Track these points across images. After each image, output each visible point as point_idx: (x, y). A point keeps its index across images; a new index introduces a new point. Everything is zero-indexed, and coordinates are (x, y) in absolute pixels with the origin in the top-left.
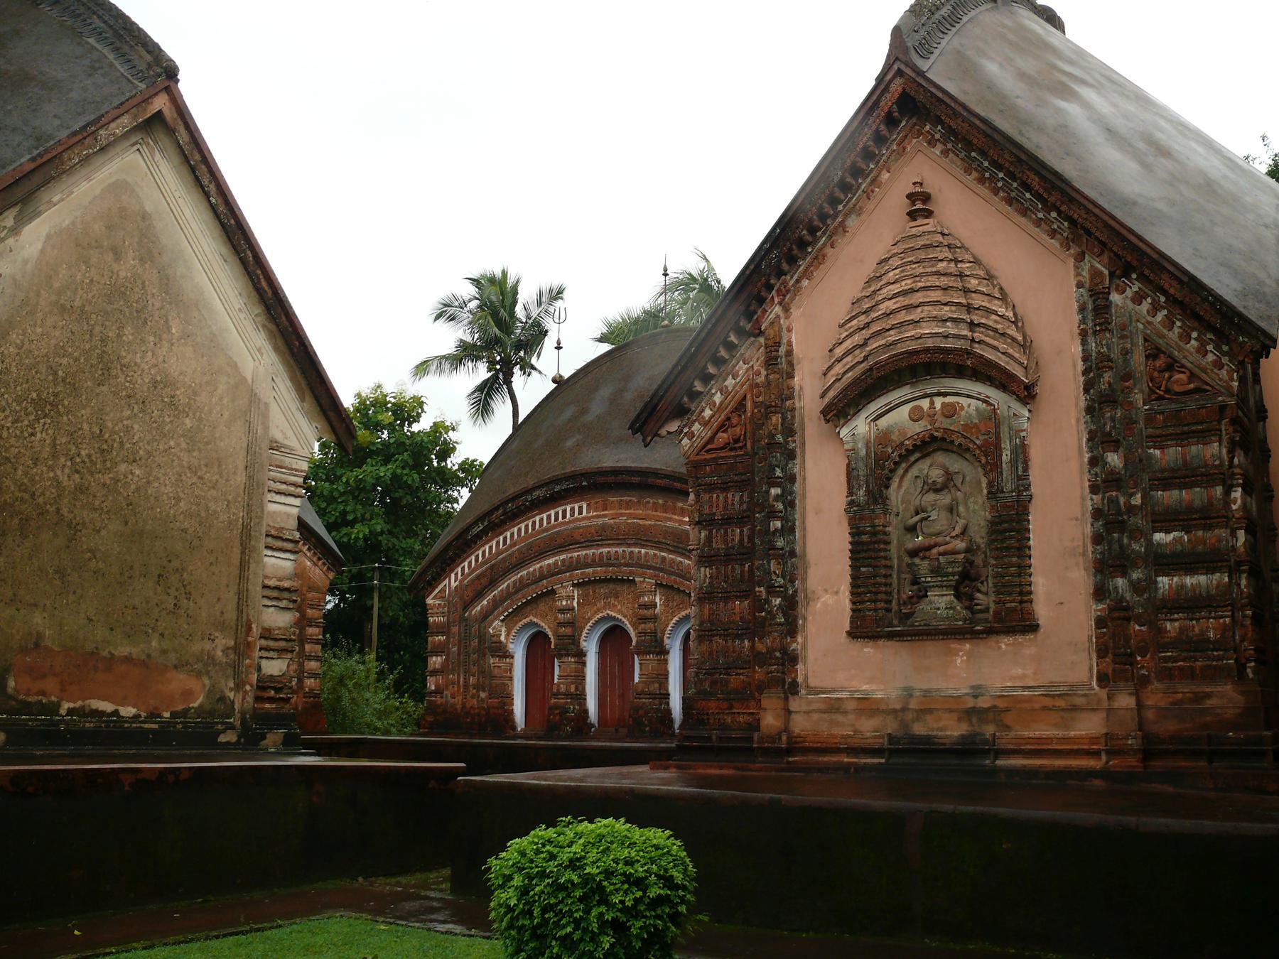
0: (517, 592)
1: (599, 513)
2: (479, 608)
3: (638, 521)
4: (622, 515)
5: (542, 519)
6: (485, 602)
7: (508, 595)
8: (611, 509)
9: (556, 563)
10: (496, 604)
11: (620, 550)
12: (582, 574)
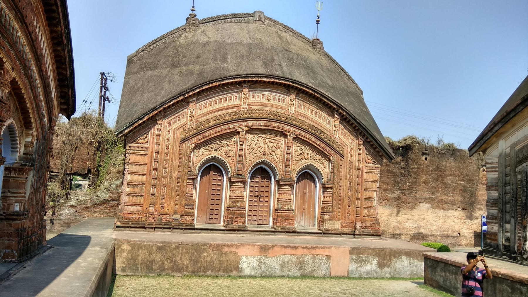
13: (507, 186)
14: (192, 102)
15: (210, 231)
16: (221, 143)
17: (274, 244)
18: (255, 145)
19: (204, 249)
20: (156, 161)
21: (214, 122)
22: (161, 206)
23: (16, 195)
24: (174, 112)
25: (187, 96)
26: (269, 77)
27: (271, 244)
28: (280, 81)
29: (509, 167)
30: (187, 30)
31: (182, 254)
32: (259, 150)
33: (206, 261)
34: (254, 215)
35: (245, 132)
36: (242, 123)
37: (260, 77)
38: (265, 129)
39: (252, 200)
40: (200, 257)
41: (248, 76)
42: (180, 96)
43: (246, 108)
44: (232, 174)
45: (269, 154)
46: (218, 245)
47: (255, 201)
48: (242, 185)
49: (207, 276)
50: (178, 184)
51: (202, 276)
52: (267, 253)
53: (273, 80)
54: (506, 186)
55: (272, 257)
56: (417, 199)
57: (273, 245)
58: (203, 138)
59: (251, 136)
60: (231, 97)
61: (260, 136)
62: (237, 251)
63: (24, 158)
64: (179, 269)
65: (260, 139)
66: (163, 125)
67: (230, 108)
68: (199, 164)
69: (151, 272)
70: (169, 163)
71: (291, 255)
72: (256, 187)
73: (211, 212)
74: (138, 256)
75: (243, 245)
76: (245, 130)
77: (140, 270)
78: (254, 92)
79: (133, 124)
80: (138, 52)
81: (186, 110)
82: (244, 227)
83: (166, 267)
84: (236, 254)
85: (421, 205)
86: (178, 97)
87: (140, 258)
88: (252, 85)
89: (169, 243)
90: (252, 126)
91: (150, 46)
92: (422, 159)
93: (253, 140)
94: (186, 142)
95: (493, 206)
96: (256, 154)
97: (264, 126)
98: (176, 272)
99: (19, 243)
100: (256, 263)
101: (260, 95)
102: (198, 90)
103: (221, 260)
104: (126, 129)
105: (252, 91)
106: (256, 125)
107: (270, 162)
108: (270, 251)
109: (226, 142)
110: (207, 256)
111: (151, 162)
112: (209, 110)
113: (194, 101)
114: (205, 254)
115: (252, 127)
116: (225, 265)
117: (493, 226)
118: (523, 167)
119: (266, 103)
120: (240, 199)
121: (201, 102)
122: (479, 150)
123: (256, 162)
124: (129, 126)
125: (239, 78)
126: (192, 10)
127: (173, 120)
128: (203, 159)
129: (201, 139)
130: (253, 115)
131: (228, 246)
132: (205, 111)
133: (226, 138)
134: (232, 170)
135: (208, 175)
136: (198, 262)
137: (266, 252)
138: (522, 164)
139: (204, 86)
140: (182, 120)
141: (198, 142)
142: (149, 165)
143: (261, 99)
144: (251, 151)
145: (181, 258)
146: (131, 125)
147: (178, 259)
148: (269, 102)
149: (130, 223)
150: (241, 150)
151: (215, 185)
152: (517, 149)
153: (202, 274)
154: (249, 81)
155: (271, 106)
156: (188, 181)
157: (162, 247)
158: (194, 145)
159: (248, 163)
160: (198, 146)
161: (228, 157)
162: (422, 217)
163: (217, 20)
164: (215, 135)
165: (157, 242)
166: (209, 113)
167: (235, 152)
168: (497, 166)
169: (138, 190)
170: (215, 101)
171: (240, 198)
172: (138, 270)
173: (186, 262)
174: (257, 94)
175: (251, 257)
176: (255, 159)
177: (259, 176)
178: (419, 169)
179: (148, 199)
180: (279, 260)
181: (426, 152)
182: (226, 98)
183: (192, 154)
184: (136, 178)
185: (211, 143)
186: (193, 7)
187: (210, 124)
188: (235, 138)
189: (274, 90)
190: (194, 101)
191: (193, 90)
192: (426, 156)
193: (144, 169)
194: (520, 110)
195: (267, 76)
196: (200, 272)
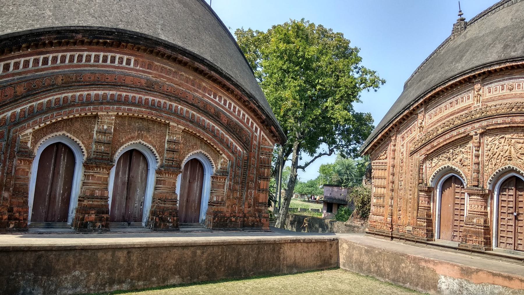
0: (61, 108)
1: (144, 69)
2: (9, 114)
3: (174, 85)
4: (163, 77)
5: (90, 56)
6: (18, 110)
7: (49, 109)
8: (155, 70)
9: (105, 96)
10: (32, 114)
11: (163, 101)
12: (128, 110)
14: (420, 113)
15: (441, 248)
16: (455, 151)
17: (479, 268)
18: (497, 149)
19: (402, 259)
20: (393, 175)
21: (443, 129)
22: (398, 217)
23: (216, 192)
24: (407, 126)
25: (412, 108)
26: (502, 63)
27: (473, 267)
28: (519, 63)
30: (452, 38)
31: (384, 261)
32: (502, 154)
33: (405, 272)
34: (508, 237)
35: (479, 135)
36: (473, 125)
37: (490, 66)
38: (505, 127)
39: (504, 217)
40: (399, 267)
41: (473, 70)
42: (405, 110)
43: (479, 106)
44: (468, 186)
45: (517, 158)
46: (415, 259)
47: (508, 219)
48: (479, 198)
49: (405, 288)
50: (411, 197)
51: (401, 287)
52: (470, 277)
53: (508, 64)
55: (476, 284)
57: (477, 269)
58: (432, 148)
59: (490, 139)
60: (462, 98)
61: (503, 137)
62: (435, 268)
63: (221, 171)
64: (382, 274)
65: (502, 140)
66: (397, 141)
67: (463, 111)
68: (432, 176)
69: (361, 271)
70: (404, 176)
71: (503, 287)
72: (509, 201)
73: (456, 229)
74: (353, 255)
75: (441, 263)
76: (478, 132)
77: (354, 268)
78: (490, 86)
79: (370, 143)
80: (412, 76)
81: (417, 122)
82: (480, 249)
83: (372, 270)
84: (434, 271)
86: (404, 111)
87: (354, 257)
88: (486, 77)
89: (374, 248)
90: (487, 126)
91: (422, 66)
93: (493, 143)
94: (415, 154)
96: (498, 159)
97: (502, 124)
98: (380, 276)
99: (214, 219)
100: (456, 287)
101: (498, 87)
102: (422, 100)
103: (419, 274)
104: (366, 148)
105: (487, 84)
106: (492, 125)
107: (517, 168)
108: (473, 275)
109: (461, 149)
110: (406, 267)
111: (389, 176)
112: (438, 118)
113: (422, 111)
114: (403, 265)
115: (487, 128)
116: (423, 280)
119: (505, 95)
120: (476, 214)
121: (430, 111)
123: (498, 169)
124: (368, 146)
125: (464, 74)
126: (459, 15)
127: (406, 134)
128: (436, 170)
129: (430, 150)
130: (488, 113)
131: (426, 261)
132: (435, 120)
133: (460, 145)
134: (468, 181)
135: (450, 188)
136: (398, 271)
137: (469, 276)
139: (427, 94)
140: (414, 133)
141: (428, 153)
142: (387, 178)
143: (499, 92)
144: (491, 156)
145: (384, 264)
146: (369, 144)
147: (381, 264)
148: (511, 93)
149: (375, 230)
150: (477, 156)
151: (459, 198)
153: (401, 284)
154: (479, 75)
155: (514, 97)
156: (420, 193)
157: (369, 251)
158: (423, 157)
159: (487, 172)
160: (428, 157)
161: (464, 166)
163: (487, 13)
164: (445, 143)
165: (365, 246)
166: (438, 121)
167: (470, 159)
169: (381, 201)
170: (445, 106)
171: (477, 213)
172: (353, 267)
173: (388, 270)
174: (494, 86)
175: (450, 277)
176: (497, 166)
177: (513, 188)
179: (387, 209)
180: (485, 288)
182: (457, 101)
183: (424, 165)
184: (381, 191)
185: (444, 152)
186: (460, 11)
187: (438, 132)
188: (470, 144)
189: (516, 76)
190: (422, 111)
191: (417, 101)
193: (383, 182)
195: (499, 63)
196: (399, 282)
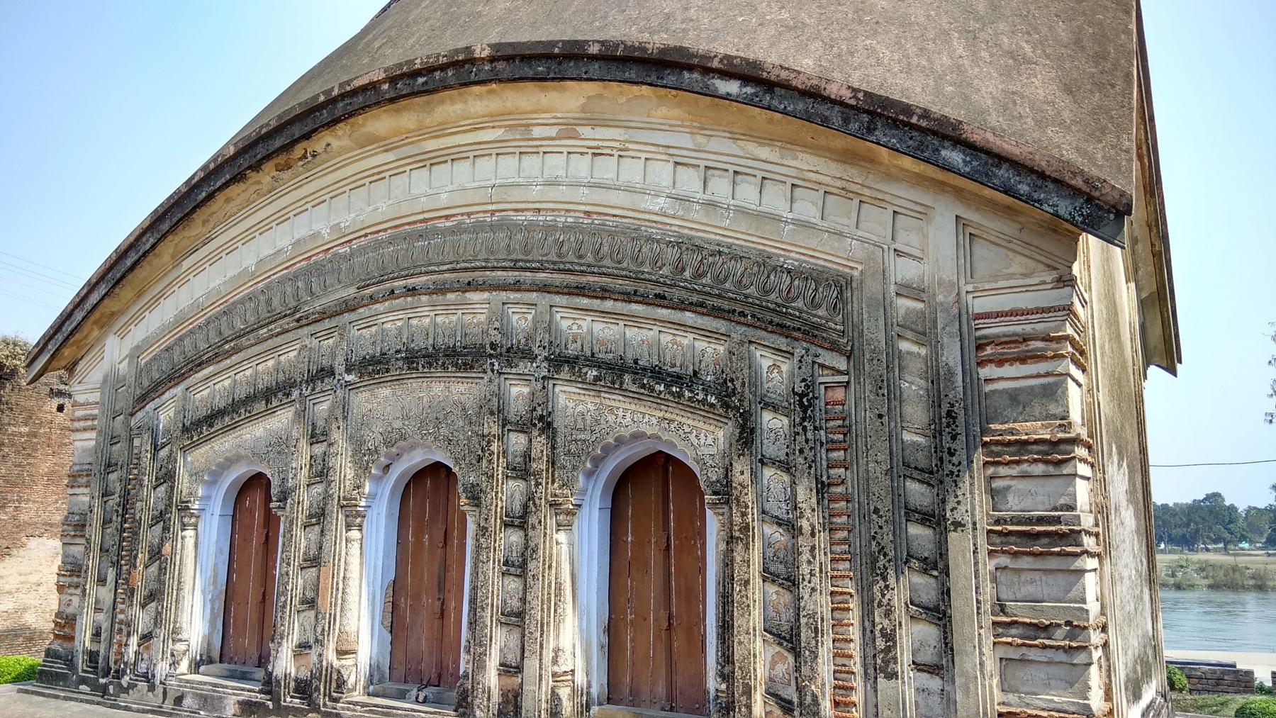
13: (113, 472)
29: (122, 416)
54: (108, 473)
56: (20, 527)
85: (33, 543)
92: (47, 408)
95: (77, 533)
117: (71, 595)
118: (148, 413)
122: (54, 364)
138: (143, 407)
152: (143, 361)
162: (34, 579)
168: (96, 412)
178: (36, 437)
181: (62, 387)
192: (61, 401)
194: (148, 246)
